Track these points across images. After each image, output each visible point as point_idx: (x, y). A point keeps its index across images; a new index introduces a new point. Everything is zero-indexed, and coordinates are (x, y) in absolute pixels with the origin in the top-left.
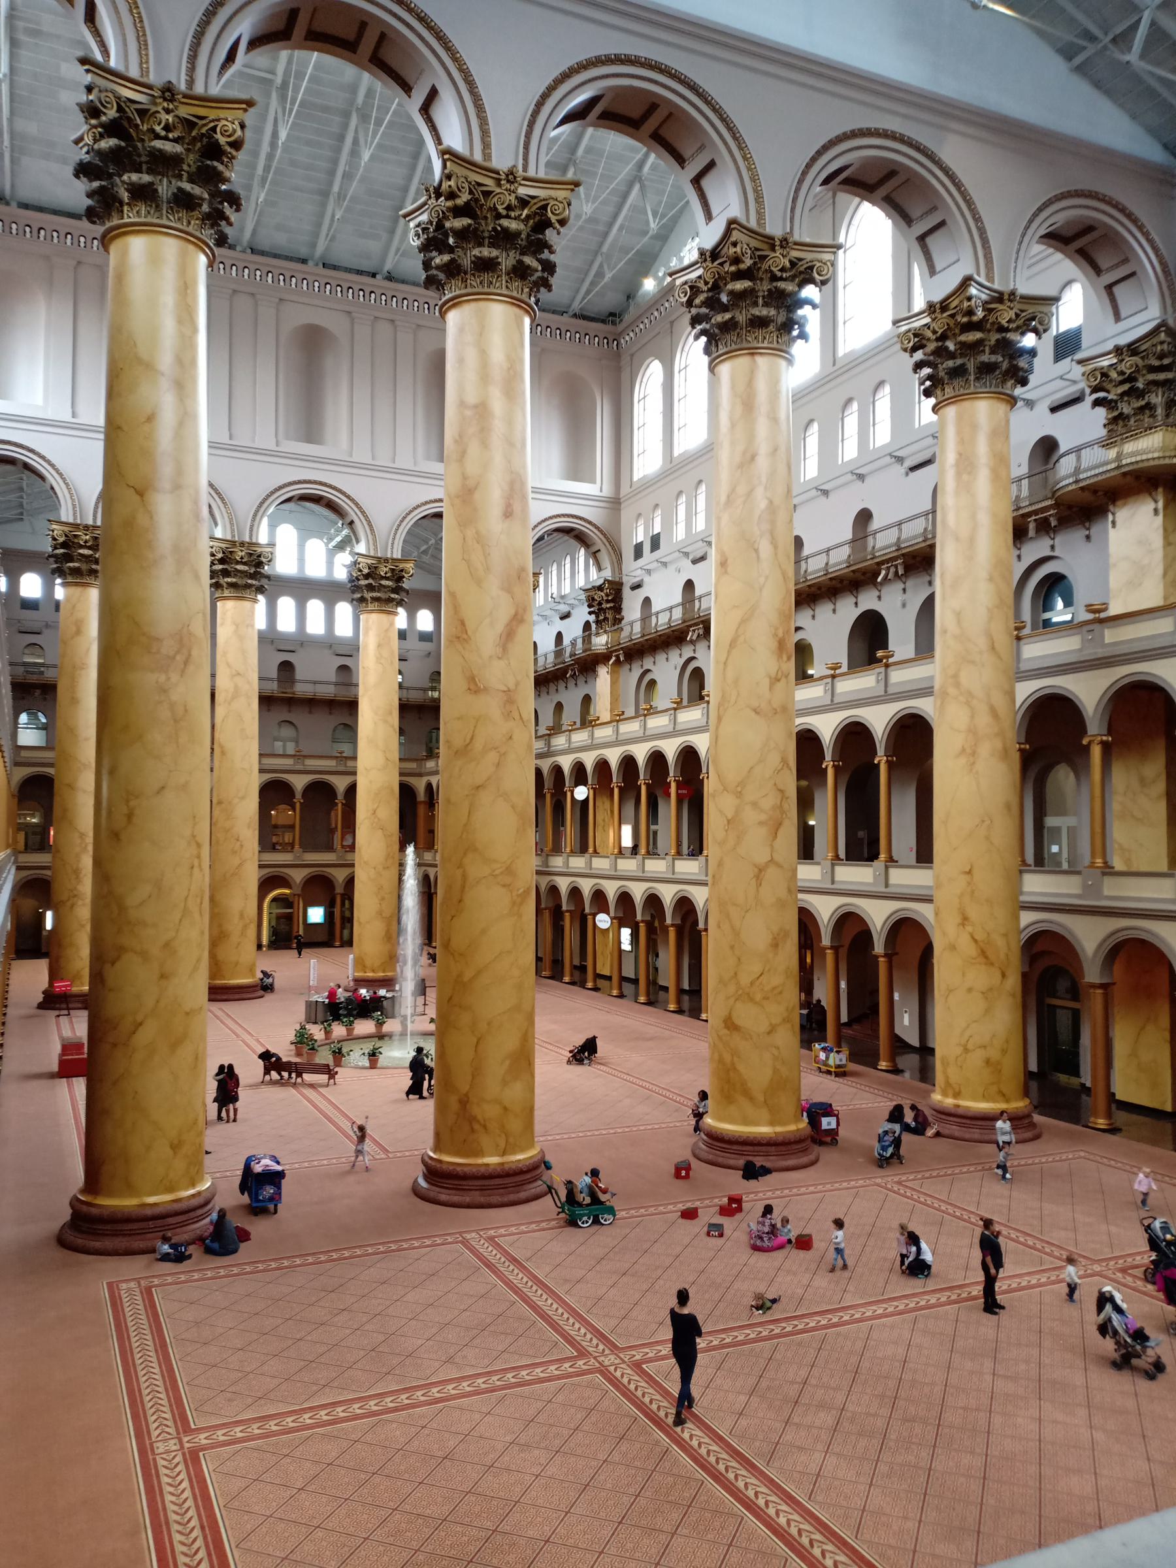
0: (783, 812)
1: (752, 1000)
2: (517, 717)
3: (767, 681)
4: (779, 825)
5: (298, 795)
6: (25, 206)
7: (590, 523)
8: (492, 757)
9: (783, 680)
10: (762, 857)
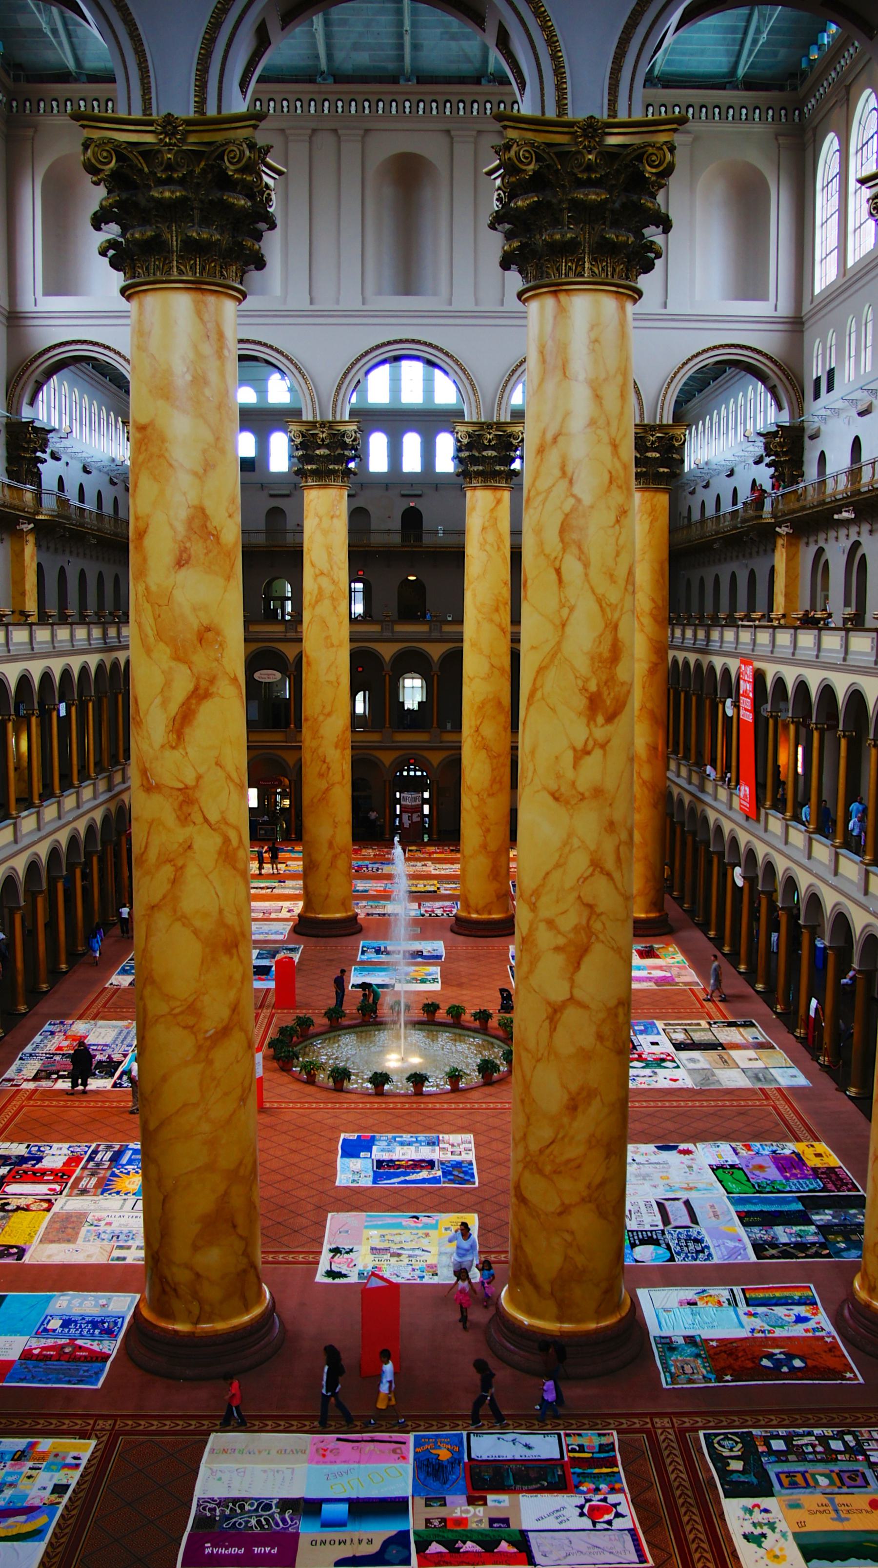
1: (540, 1171)
2: (199, 819)
3: (569, 756)
7: (759, 352)
8: (167, 871)
9: (597, 753)
10: (558, 992)
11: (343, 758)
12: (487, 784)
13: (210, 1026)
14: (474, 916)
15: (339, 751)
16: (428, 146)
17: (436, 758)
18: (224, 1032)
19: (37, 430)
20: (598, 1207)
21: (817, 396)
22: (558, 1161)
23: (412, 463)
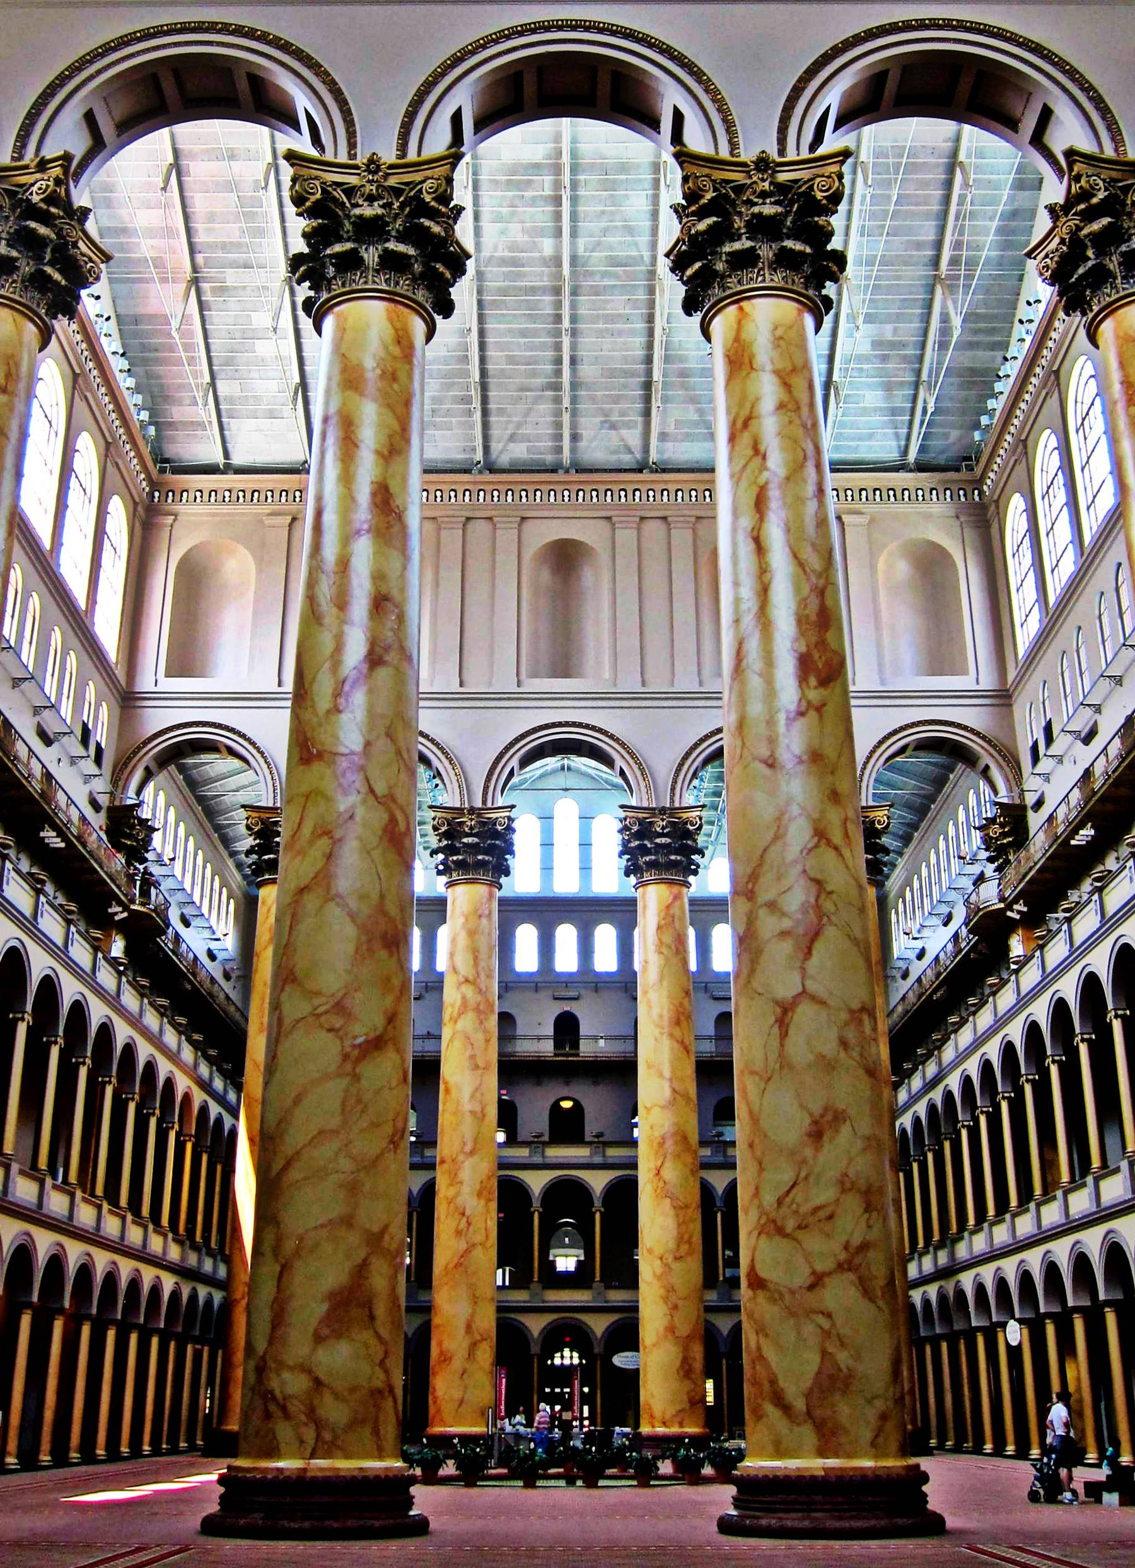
0: (820, 912)
1: (780, 1231)
4: (815, 935)
10: (787, 986)
11: (488, 1211)
12: (672, 1245)
13: (360, 1031)
14: (661, 1430)
15: (483, 1202)
17: (599, 1325)
18: (376, 1044)
20: (861, 1279)
21: (1036, 759)
22: (803, 1210)
23: (566, 960)
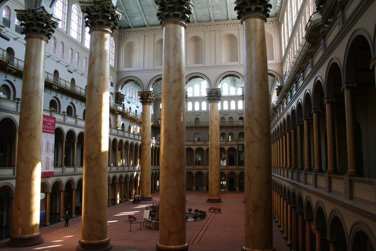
5: (226, 151)
6: (135, 27)
16: (200, 34)
19: (121, 95)
